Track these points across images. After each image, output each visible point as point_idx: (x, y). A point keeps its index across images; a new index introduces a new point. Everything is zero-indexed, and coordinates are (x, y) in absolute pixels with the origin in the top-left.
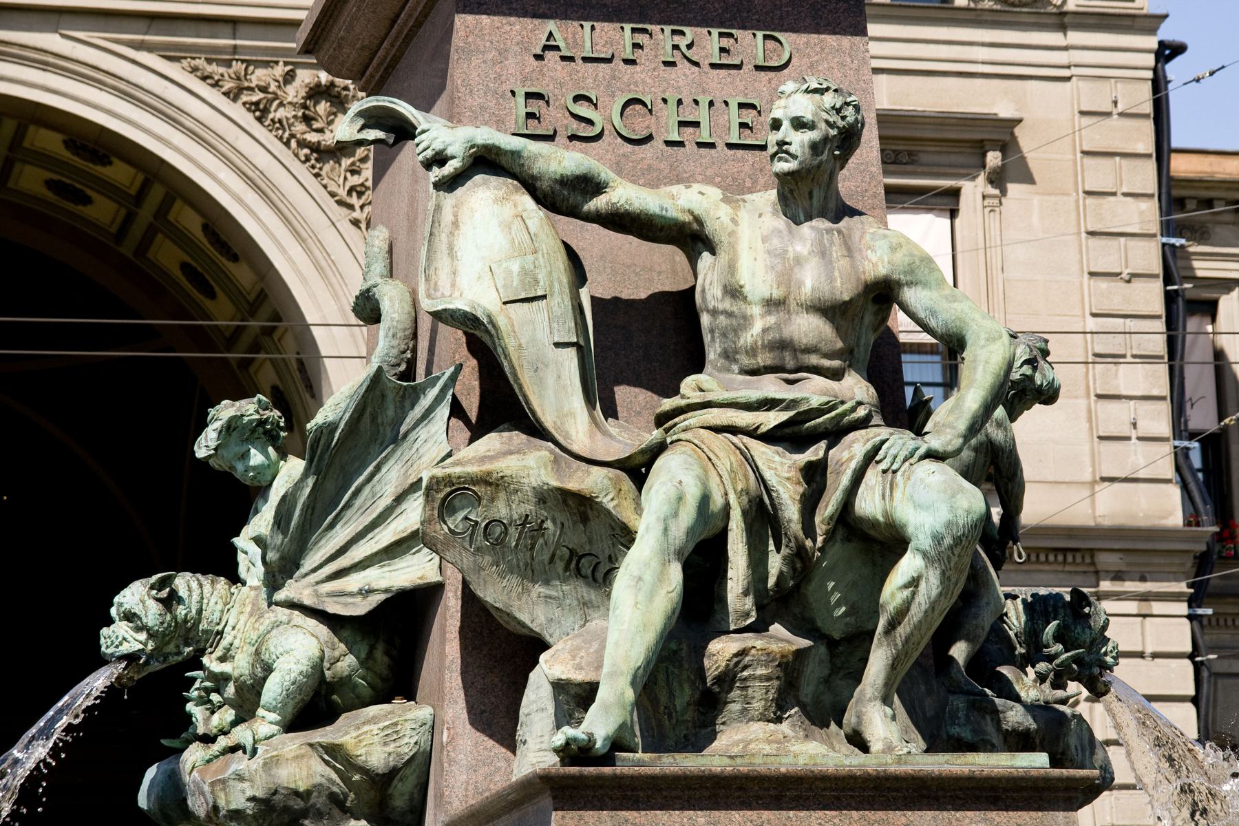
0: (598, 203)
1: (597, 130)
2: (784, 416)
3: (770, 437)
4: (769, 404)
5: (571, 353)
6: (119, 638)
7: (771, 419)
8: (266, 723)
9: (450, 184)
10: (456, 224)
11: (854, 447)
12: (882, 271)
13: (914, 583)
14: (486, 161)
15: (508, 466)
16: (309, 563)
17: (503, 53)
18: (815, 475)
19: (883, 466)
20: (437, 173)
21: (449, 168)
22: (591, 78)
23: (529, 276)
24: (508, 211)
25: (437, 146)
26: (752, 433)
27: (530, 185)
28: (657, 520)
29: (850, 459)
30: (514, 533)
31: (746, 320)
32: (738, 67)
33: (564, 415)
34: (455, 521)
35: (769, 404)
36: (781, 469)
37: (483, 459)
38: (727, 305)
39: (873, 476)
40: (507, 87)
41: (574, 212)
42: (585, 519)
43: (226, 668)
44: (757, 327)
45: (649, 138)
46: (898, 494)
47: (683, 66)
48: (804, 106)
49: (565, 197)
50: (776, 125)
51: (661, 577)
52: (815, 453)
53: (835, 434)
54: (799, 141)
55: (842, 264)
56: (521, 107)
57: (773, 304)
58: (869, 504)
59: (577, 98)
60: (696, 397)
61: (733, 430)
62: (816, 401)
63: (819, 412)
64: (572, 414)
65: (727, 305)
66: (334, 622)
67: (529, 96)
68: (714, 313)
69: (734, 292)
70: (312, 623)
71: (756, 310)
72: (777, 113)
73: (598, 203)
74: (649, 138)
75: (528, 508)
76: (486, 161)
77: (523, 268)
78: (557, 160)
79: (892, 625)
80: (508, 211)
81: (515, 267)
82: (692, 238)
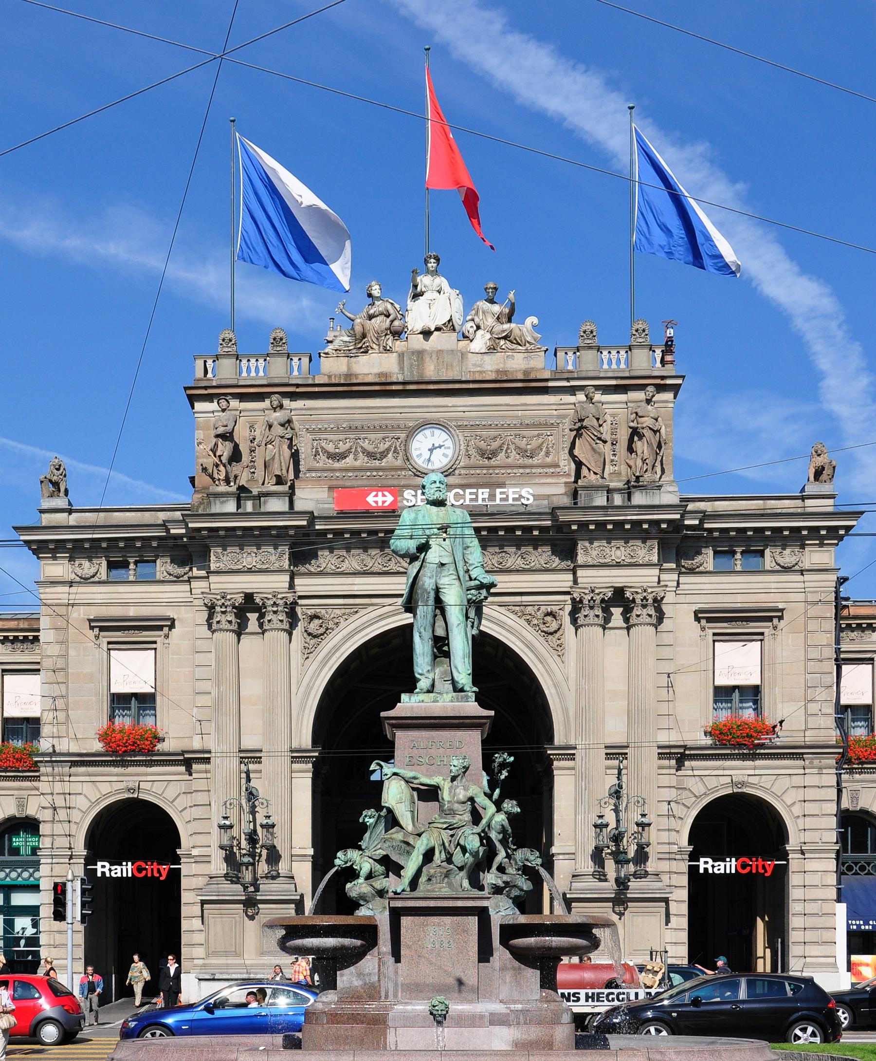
3: (446, 829)
6: (337, 862)
7: (445, 826)
8: (361, 880)
15: (394, 836)
23: (401, 798)
28: (421, 846)
33: (407, 825)
34: (386, 845)
36: (446, 835)
39: (463, 837)
48: (455, 762)
51: (417, 859)
57: (449, 802)
66: (374, 860)
69: (443, 799)
76: (395, 774)
78: (409, 774)
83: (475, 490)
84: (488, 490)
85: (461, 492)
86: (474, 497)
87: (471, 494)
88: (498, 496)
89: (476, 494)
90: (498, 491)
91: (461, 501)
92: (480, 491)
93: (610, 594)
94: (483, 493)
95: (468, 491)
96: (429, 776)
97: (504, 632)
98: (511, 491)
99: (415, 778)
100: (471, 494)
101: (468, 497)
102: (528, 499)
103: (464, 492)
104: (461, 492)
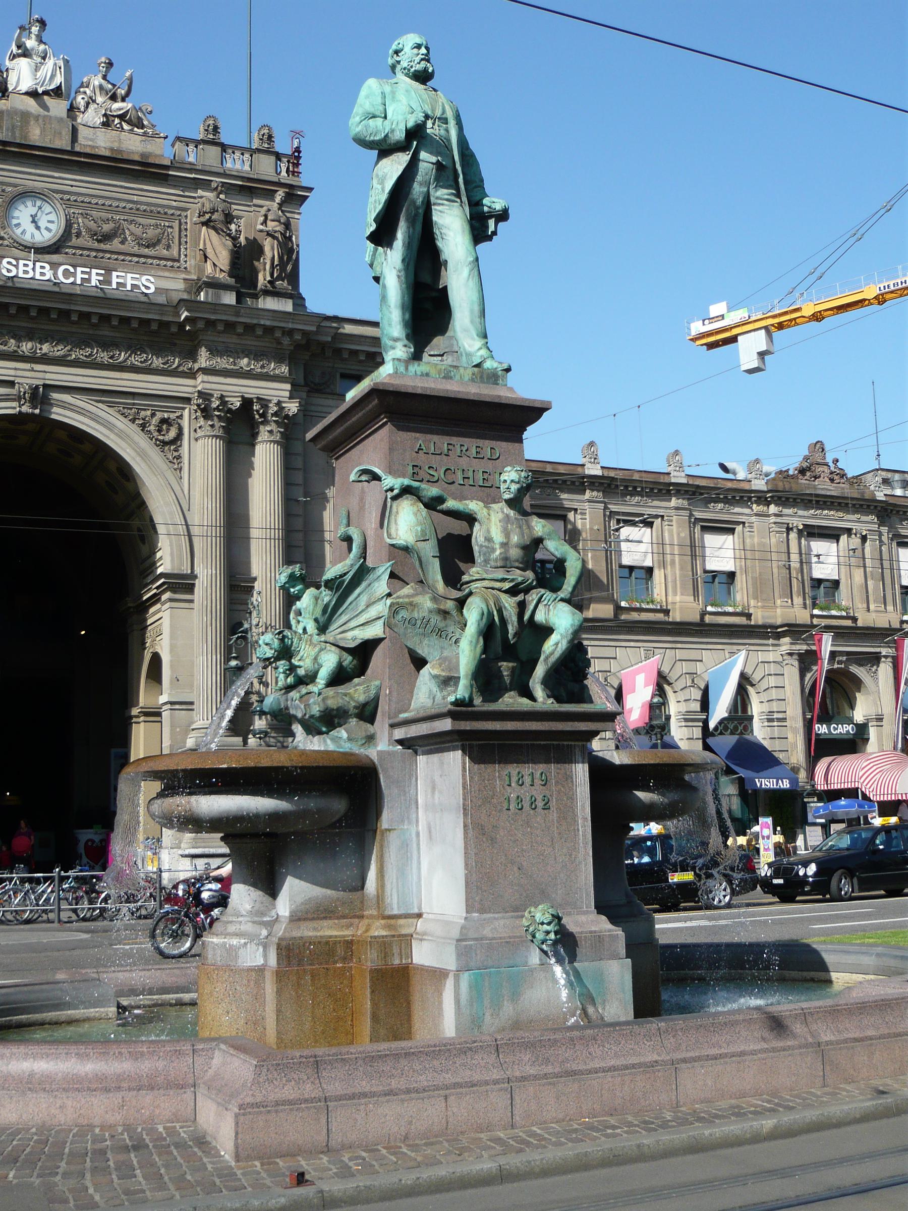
0: (444, 506)
1: (436, 479)
2: (511, 584)
3: (506, 592)
4: (503, 580)
5: (437, 559)
7: (507, 586)
9: (394, 498)
10: (397, 512)
11: (533, 597)
12: (540, 534)
13: (557, 644)
14: (406, 491)
16: (332, 628)
17: (405, 451)
18: (522, 606)
19: (545, 602)
20: (390, 495)
21: (396, 492)
22: (435, 460)
24: (415, 509)
25: (391, 485)
26: (500, 590)
27: (420, 499)
29: (533, 600)
30: (419, 622)
31: (494, 550)
32: (483, 458)
35: (503, 580)
36: (509, 604)
37: (408, 596)
38: (486, 544)
40: (406, 463)
41: (435, 509)
42: (445, 618)
43: (301, 663)
44: (498, 552)
45: (454, 482)
46: (551, 613)
47: (465, 458)
49: (433, 504)
50: (505, 481)
52: (520, 597)
53: (527, 591)
54: (514, 487)
55: (526, 531)
56: (410, 470)
58: (540, 617)
59: (429, 468)
60: (477, 576)
61: (493, 589)
62: (520, 579)
63: (522, 583)
64: (437, 581)
65: (486, 544)
67: (413, 466)
68: (481, 546)
69: (489, 539)
70: (333, 648)
71: (498, 546)
72: (506, 478)
73: (444, 506)
74: (454, 482)
75: (426, 614)
77: (422, 531)
79: (547, 658)
80: (415, 509)
81: (419, 529)
82: (470, 519)
83: (88, 270)
84: (103, 272)
85: (72, 270)
86: (86, 276)
87: (83, 272)
88: (115, 280)
89: (89, 273)
90: (114, 274)
91: (71, 280)
92: (94, 271)
93: (238, 404)
94: (95, 277)
95: (79, 269)
96: (461, 498)
97: (112, 436)
98: (129, 275)
99: (440, 500)
100: (83, 272)
101: (79, 276)
102: (147, 288)
103: (75, 270)
104: (72, 270)
